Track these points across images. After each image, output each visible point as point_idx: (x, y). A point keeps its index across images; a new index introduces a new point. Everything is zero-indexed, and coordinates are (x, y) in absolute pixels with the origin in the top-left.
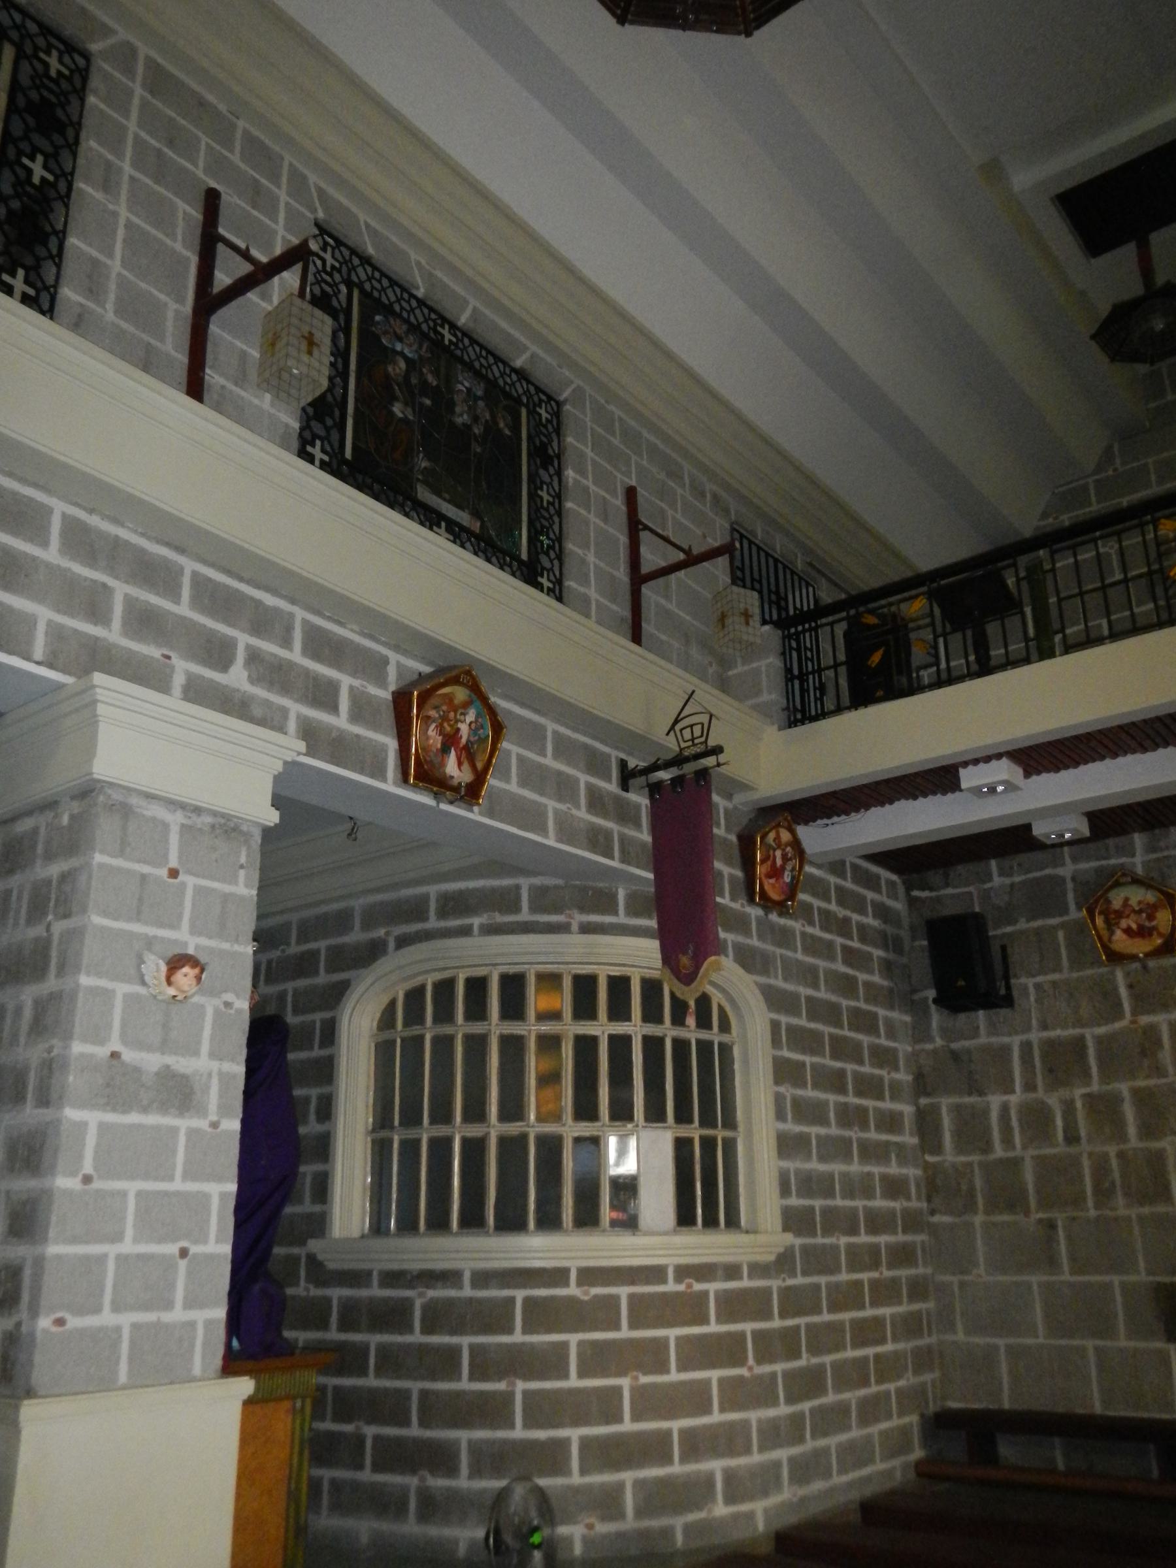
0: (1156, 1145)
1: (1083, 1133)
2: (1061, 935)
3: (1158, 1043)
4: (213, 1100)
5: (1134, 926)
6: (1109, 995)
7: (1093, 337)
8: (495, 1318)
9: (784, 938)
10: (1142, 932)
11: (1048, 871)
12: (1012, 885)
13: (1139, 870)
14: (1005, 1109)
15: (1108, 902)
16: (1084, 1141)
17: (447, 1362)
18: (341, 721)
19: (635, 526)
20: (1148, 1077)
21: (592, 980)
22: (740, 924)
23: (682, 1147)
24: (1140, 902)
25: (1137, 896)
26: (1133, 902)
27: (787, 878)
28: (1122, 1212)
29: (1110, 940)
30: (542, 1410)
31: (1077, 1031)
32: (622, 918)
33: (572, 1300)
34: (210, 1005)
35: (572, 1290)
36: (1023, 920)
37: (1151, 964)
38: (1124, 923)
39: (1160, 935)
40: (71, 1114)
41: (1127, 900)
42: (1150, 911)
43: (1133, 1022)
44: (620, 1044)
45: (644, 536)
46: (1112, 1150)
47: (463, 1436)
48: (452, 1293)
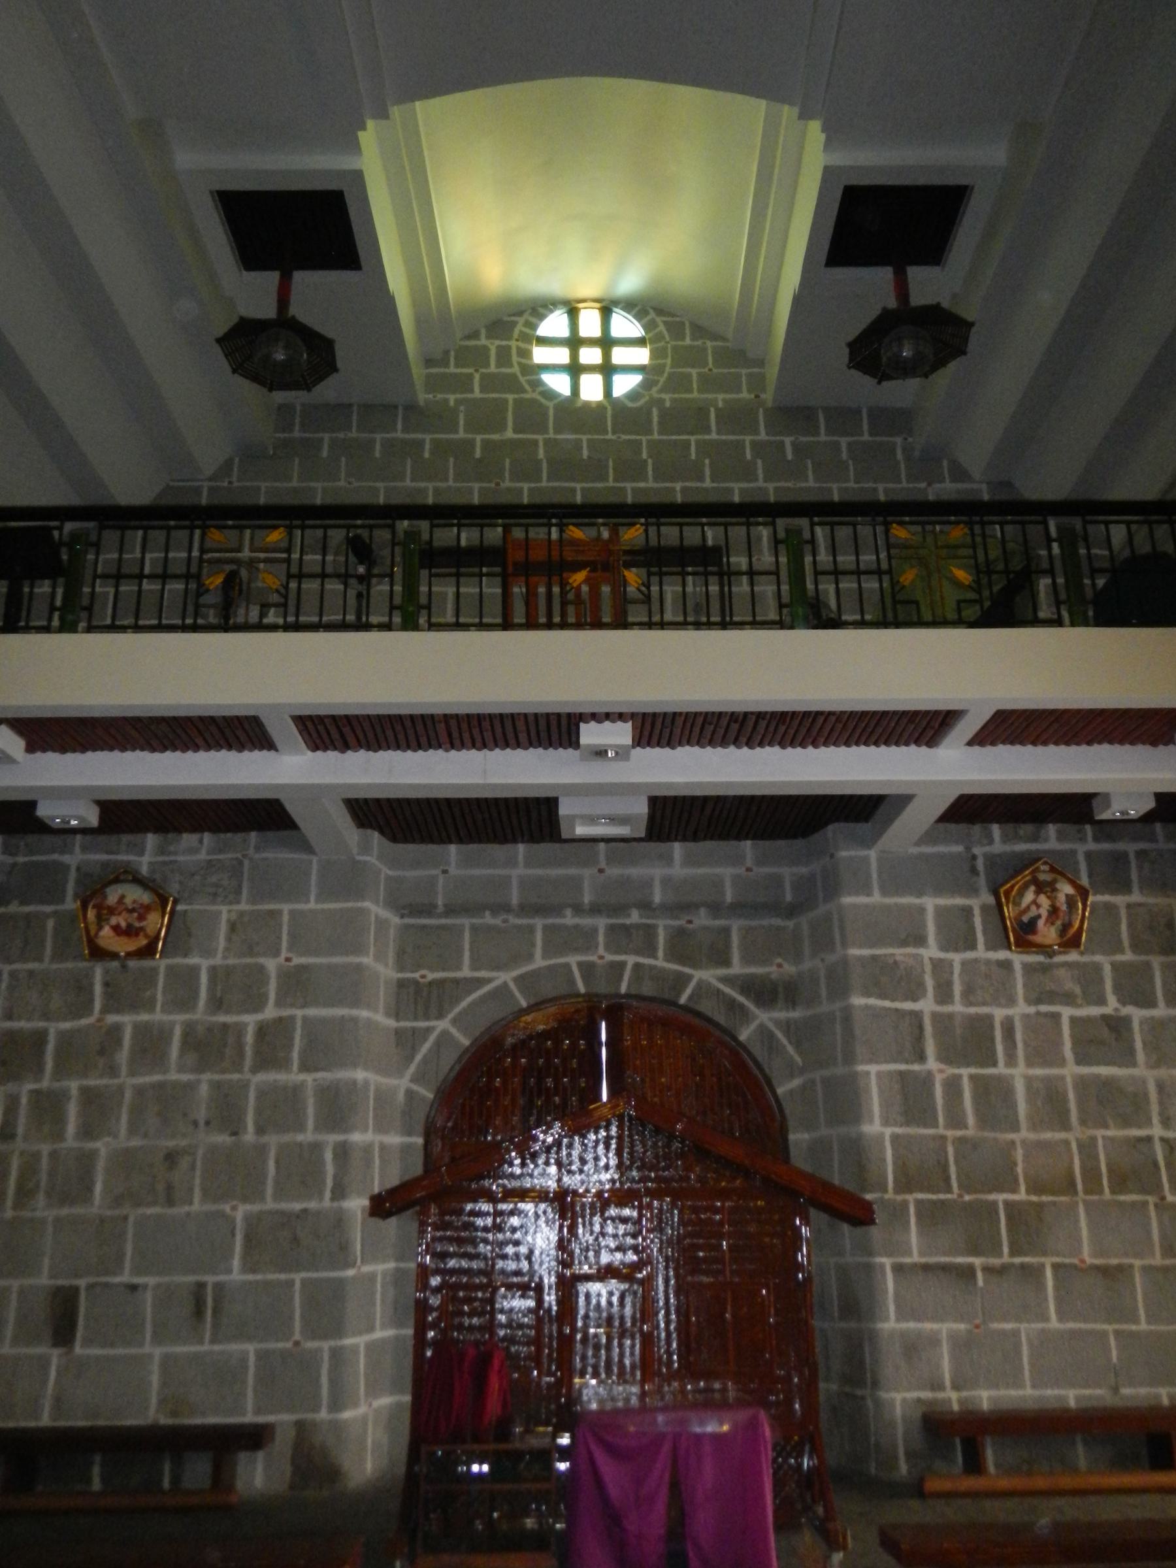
0: (91, 1145)
1: (20, 1130)
2: (50, 924)
3: (119, 1042)
5: (123, 924)
6: (83, 988)
7: (219, 341)
10: (129, 932)
11: (55, 856)
12: (15, 865)
13: (144, 870)
15: (105, 897)
16: (19, 1139)
20: (101, 1076)
24: (134, 902)
25: (134, 895)
26: (128, 901)
28: (38, 1214)
29: (96, 934)
31: (42, 1024)
36: (16, 902)
37: (132, 964)
38: (114, 920)
39: (146, 936)
41: (122, 897)
42: (142, 911)
43: (99, 1020)
46: (45, 1149)
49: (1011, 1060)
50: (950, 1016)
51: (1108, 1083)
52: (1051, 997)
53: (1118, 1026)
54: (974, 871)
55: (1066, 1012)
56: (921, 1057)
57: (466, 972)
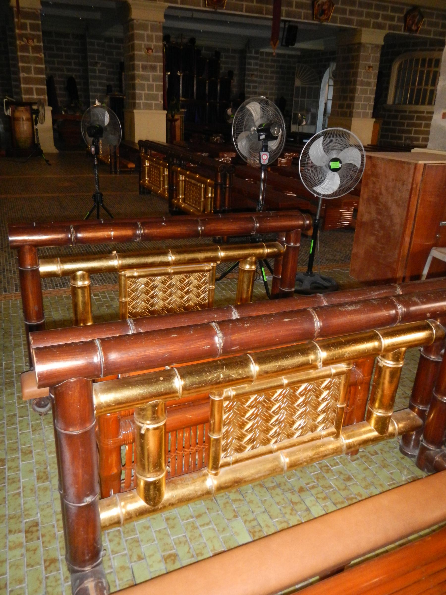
4: (373, 85)
8: (412, 118)
17: (403, 124)
18: (395, 23)
30: (416, 132)
33: (424, 117)
34: (373, 72)
35: (425, 115)
47: (404, 135)
48: (405, 114)
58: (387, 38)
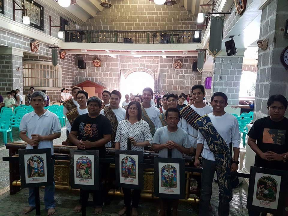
9: (63, 62)
10: (97, 64)
14: (84, 78)
19: (50, 21)
21: (45, 65)
22: (59, 61)
23: (53, 80)
25: (98, 61)
27: (64, 56)
31: (91, 72)
32: (48, 60)
40: (13, 78)
44: (48, 71)
45: (51, 22)
49: (173, 79)
50: (168, 75)
51: (182, 81)
52: (178, 73)
53: (184, 76)
54: (173, 61)
55: (179, 74)
56: (165, 78)
57: (127, 69)
58: (24, 53)
